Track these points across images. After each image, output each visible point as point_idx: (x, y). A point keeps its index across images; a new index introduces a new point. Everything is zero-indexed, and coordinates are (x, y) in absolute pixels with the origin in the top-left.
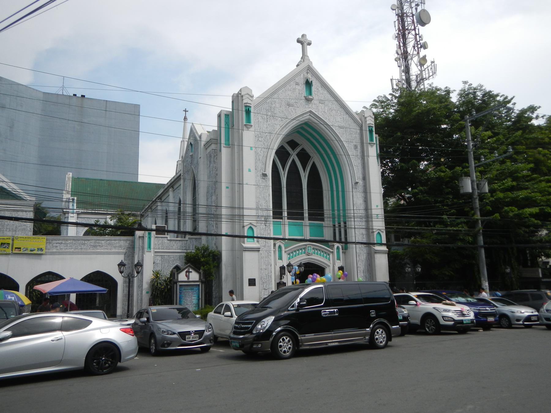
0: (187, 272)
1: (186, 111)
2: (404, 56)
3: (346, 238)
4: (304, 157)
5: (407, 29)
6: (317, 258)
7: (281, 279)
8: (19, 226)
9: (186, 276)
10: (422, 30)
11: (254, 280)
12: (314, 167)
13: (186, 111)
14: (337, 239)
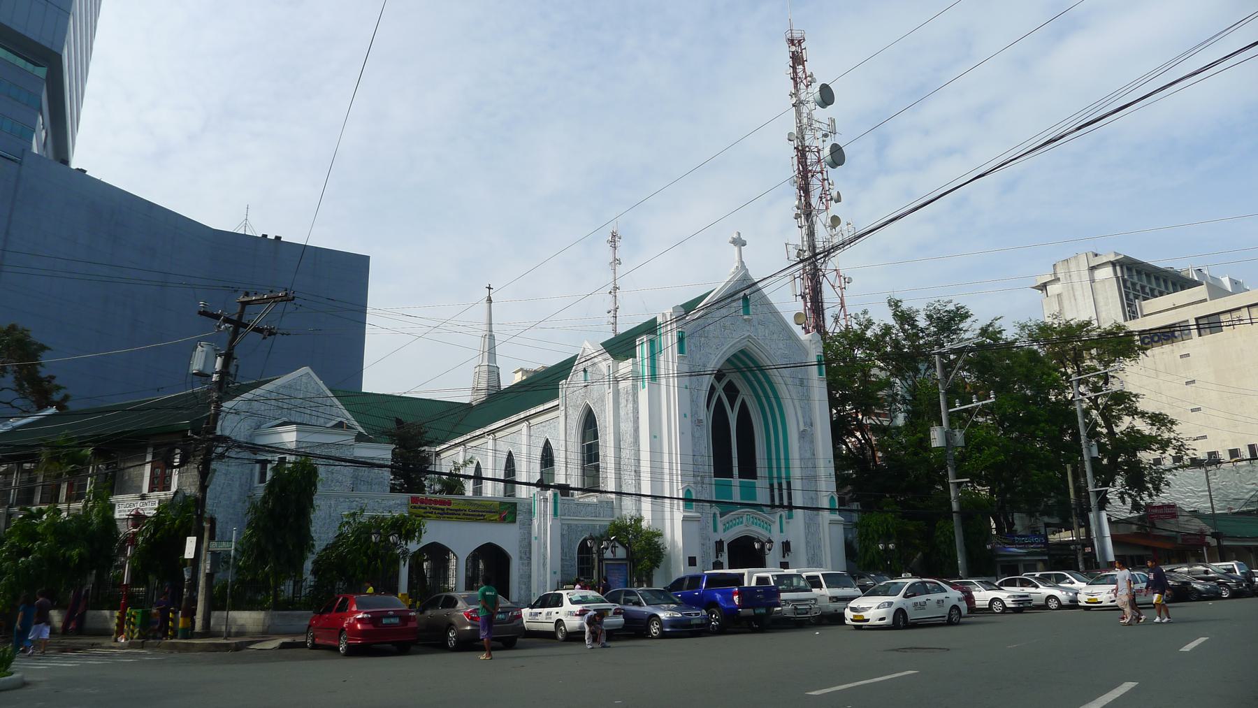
0: (612, 547)
1: (489, 288)
2: (807, 212)
3: (790, 503)
4: (732, 391)
5: (810, 171)
6: (756, 530)
7: (717, 557)
8: (376, 479)
9: (612, 552)
10: (832, 173)
11: (695, 558)
12: (743, 405)
13: (489, 288)
14: (777, 503)
